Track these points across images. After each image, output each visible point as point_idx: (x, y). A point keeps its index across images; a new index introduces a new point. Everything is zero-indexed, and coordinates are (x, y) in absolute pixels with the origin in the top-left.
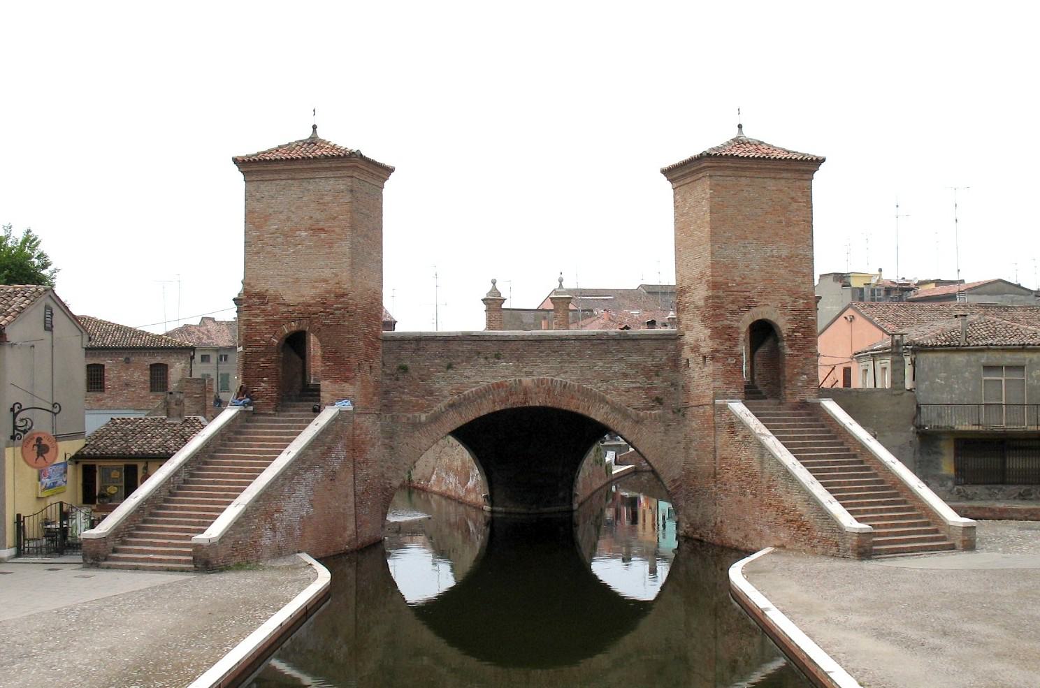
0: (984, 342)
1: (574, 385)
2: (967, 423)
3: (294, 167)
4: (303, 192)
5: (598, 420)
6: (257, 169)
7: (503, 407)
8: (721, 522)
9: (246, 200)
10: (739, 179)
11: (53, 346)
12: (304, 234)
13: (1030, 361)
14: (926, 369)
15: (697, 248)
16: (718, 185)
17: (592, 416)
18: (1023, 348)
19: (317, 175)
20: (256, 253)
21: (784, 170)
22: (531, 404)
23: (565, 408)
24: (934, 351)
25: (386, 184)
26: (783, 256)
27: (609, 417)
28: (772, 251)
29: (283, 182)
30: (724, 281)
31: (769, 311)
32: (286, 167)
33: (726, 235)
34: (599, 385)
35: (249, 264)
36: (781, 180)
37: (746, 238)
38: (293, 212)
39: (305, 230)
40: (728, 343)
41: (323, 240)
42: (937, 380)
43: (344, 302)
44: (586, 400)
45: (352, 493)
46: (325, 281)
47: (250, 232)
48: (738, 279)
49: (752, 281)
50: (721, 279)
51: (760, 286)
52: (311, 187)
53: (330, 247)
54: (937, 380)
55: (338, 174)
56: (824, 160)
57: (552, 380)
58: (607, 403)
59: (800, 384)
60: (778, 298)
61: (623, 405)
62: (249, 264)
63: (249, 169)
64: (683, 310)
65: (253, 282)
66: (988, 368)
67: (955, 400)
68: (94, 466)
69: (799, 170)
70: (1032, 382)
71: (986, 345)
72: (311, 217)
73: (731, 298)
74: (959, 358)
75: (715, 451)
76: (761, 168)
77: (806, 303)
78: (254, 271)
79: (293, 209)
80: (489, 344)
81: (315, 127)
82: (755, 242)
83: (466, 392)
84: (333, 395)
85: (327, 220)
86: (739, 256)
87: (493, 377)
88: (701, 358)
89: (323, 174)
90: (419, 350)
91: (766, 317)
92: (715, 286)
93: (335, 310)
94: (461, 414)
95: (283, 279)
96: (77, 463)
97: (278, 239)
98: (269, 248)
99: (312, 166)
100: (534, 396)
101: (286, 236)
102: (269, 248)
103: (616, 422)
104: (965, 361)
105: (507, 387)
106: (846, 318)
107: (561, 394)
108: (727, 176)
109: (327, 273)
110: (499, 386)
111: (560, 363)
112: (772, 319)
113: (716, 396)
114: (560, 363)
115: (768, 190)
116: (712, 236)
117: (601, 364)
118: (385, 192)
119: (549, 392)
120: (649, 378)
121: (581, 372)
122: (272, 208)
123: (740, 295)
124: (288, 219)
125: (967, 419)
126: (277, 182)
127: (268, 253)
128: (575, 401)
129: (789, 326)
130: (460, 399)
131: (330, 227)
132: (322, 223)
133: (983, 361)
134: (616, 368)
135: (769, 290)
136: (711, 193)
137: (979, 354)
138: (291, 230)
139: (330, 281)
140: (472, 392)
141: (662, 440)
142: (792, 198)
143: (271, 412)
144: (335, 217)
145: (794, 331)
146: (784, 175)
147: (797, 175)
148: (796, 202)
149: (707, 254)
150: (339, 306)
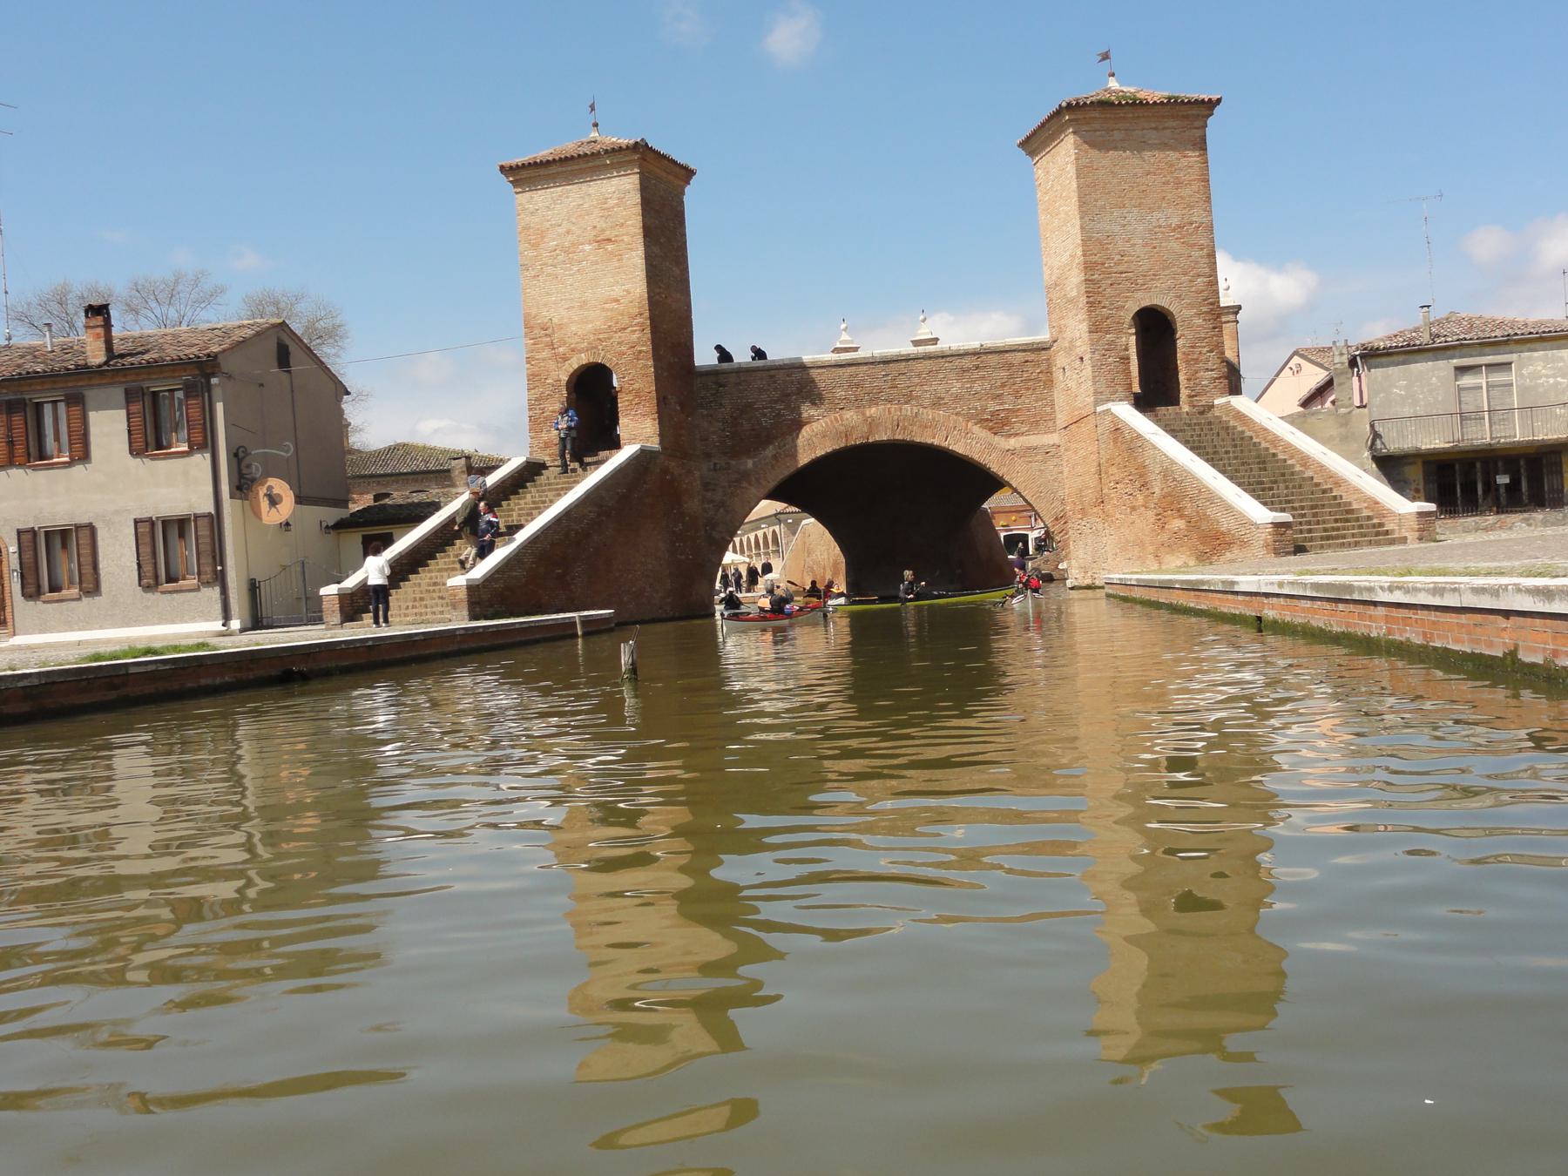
0: (1455, 338)
2: (1437, 441)
3: (569, 168)
11: (292, 391)
12: (587, 247)
14: (1380, 378)
15: (1064, 228)
18: (1508, 340)
24: (1388, 354)
25: (687, 189)
26: (1173, 226)
28: (1158, 220)
33: (1100, 203)
35: (528, 291)
39: (590, 244)
41: (611, 253)
46: (617, 301)
53: (619, 260)
56: (1219, 101)
62: (528, 291)
63: (518, 177)
65: (534, 311)
67: (1422, 413)
69: (1186, 117)
70: (1522, 381)
71: (1458, 340)
72: (595, 227)
79: (574, 220)
82: (1135, 210)
85: (612, 228)
86: (1117, 228)
92: (1089, 267)
98: (549, 269)
102: (549, 269)
106: (1291, 369)
108: (1095, 131)
109: (617, 291)
113: (1097, 403)
115: (1149, 144)
116: (1080, 206)
117: (959, 385)
118: (685, 199)
122: (548, 221)
124: (568, 232)
125: (1437, 435)
126: (552, 190)
127: (549, 275)
131: (616, 236)
132: (608, 233)
136: (1076, 153)
139: (622, 301)
141: (1040, 470)
144: (623, 224)
149: (1077, 230)
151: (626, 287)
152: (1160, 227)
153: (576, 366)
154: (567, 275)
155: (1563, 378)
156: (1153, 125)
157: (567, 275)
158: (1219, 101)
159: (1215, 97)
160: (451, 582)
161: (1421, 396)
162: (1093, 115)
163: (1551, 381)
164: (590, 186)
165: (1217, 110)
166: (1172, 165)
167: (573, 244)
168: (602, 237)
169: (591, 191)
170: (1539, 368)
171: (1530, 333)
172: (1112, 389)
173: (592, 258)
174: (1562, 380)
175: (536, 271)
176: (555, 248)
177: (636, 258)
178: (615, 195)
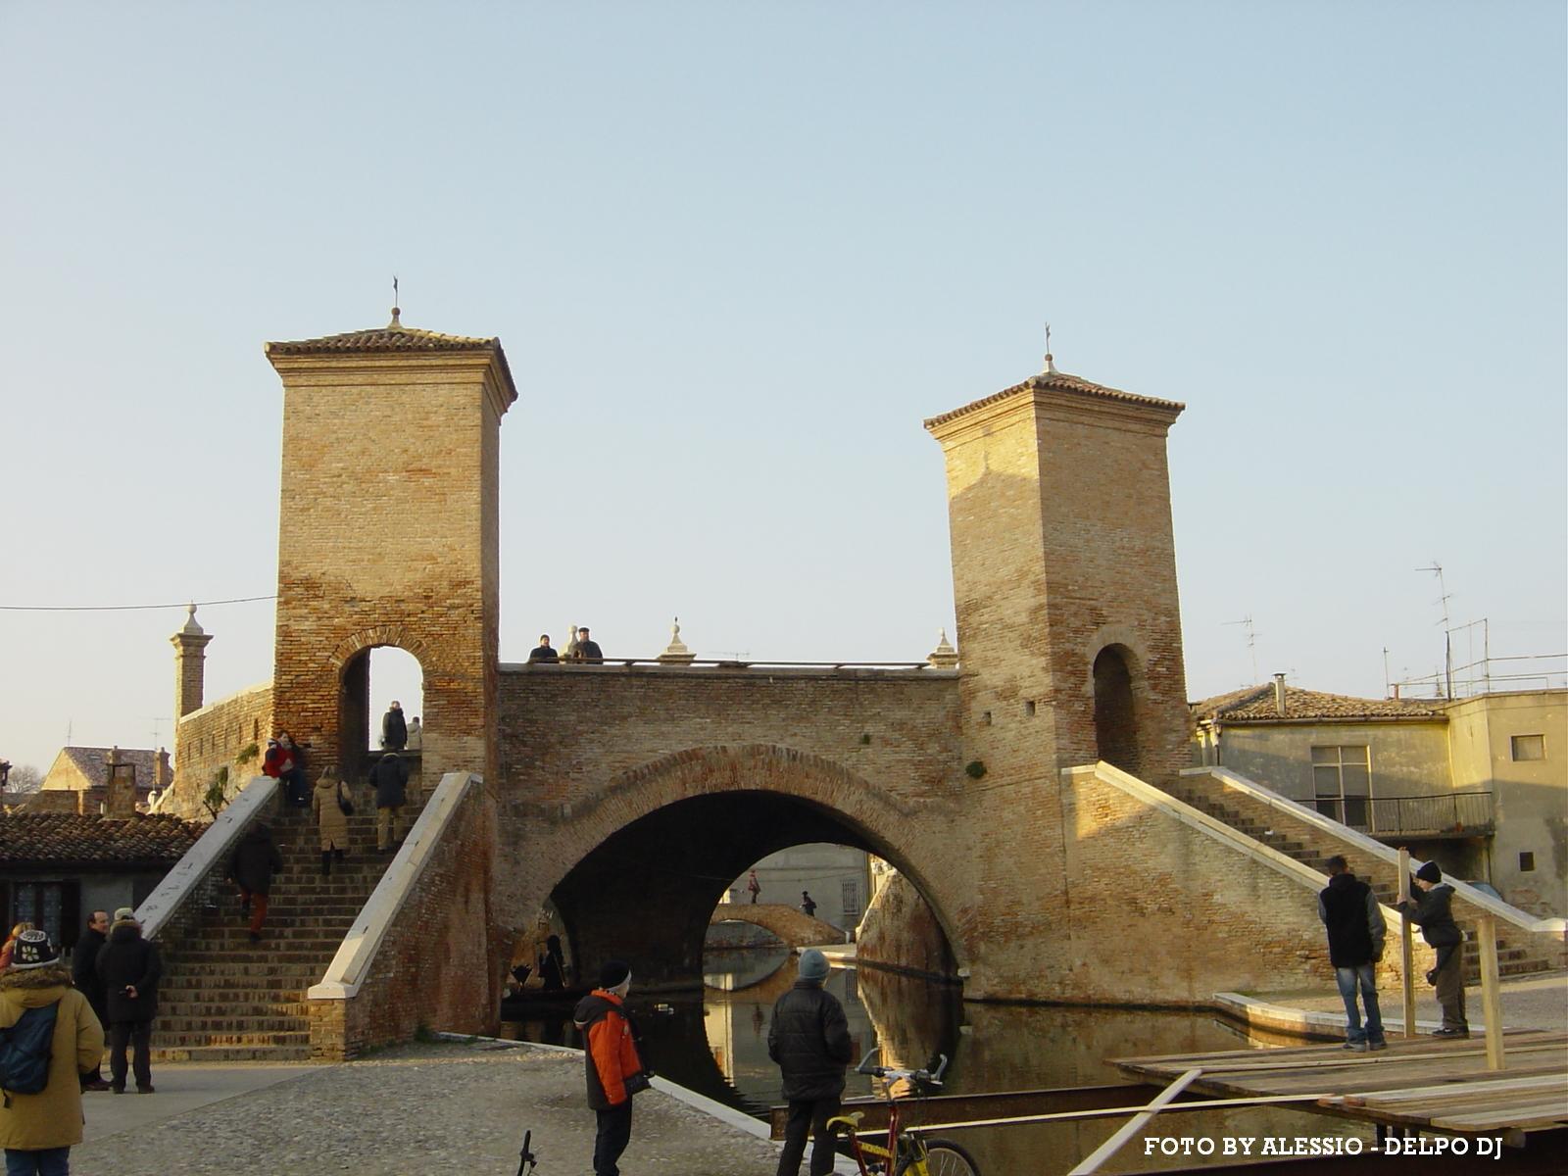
1: (808, 756)
5: (848, 812)
6: (311, 365)
7: (698, 792)
8: (1084, 965)
9: (287, 418)
10: (1074, 426)
12: (392, 478)
13: (1374, 739)
17: (839, 806)
18: (1366, 721)
19: (415, 377)
20: (302, 510)
21: (1132, 418)
22: (743, 786)
23: (796, 794)
25: (504, 418)
26: (1137, 549)
27: (865, 807)
28: (1121, 540)
29: (355, 390)
30: (1065, 581)
31: (1121, 631)
32: (369, 364)
33: (1064, 509)
34: (846, 756)
36: (1128, 434)
37: (1088, 518)
38: (374, 441)
39: (396, 472)
40: (1072, 679)
41: (430, 489)
42: (1251, 769)
43: (464, 594)
44: (828, 779)
45: (485, 933)
46: (432, 559)
47: (293, 473)
48: (1080, 580)
49: (1099, 584)
50: (1058, 578)
54: (1251, 769)
55: (458, 376)
56: (1183, 408)
57: (774, 747)
59: (1170, 747)
60: (1132, 611)
61: (884, 789)
62: (290, 528)
64: (974, 636)
69: (1149, 421)
73: (1073, 608)
75: (1065, 850)
77: (1167, 622)
78: (297, 542)
81: (396, 312)
82: (1099, 524)
84: (444, 757)
87: (680, 742)
88: (1022, 707)
89: (429, 377)
91: (1121, 640)
93: (449, 608)
94: (630, 804)
95: (354, 555)
97: (345, 486)
98: (329, 502)
99: (414, 363)
101: (359, 481)
103: (875, 815)
104: (1287, 740)
105: (704, 758)
108: (1058, 420)
109: (434, 545)
110: (690, 756)
111: (784, 720)
112: (1128, 645)
113: (1062, 763)
114: (784, 720)
117: (847, 722)
120: (921, 747)
121: (817, 733)
122: (335, 432)
123: (1084, 605)
127: (328, 510)
128: (810, 780)
129: (1150, 656)
130: (628, 778)
133: (1311, 740)
135: (1122, 599)
138: (369, 471)
148: (1147, 468)
150: (456, 601)
154: (354, 513)
155: (1416, 767)
157: (354, 513)
161: (1278, 777)
162: (1059, 402)
163: (1405, 769)
164: (404, 392)
165: (1182, 412)
168: (416, 465)
170: (1393, 755)
171: (1386, 715)
172: (1075, 746)
173: (397, 493)
174: (1416, 770)
178: (442, 410)
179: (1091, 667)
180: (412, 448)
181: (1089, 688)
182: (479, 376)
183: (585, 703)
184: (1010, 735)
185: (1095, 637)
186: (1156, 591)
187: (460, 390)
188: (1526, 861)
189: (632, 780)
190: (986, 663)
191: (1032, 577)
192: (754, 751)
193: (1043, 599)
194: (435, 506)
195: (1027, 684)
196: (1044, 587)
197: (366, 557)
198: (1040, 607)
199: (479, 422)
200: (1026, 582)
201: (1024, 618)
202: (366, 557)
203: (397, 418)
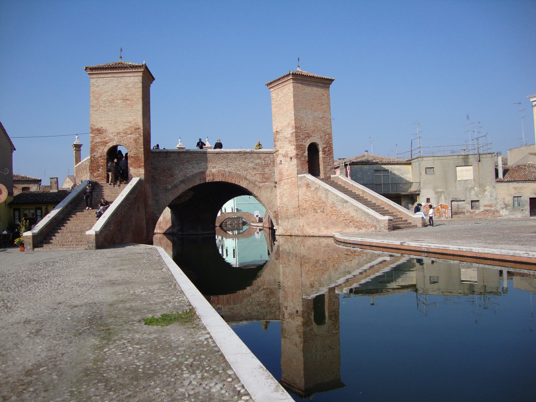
4: (119, 83)
12: (119, 101)
16: (296, 86)
21: (319, 82)
25: (152, 85)
30: (299, 126)
35: (93, 115)
39: (120, 100)
41: (129, 104)
43: (138, 132)
45: (145, 218)
46: (130, 122)
50: (298, 125)
51: (312, 129)
52: (122, 80)
55: (136, 74)
57: (224, 170)
58: (247, 180)
59: (328, 169)
60: (319, 134)
62: (93, 115)
64: (278, 141)
66: (376, 171)
68: (20, 208)
69: (324, 83)
72: (122, 94)
74: (366, 167)
76: (311, 81)
78: (95, 119)
80: (197, 155)
83: (188, 176)
88: (289, 159)
90: (167, 157)
96: (11, 208)
98: (103, 108)
100: (217, 177)
107: (229, 176)
109: (130, 119)
118: (151, 88)
119: (223, 175)
124: (111, 95)
126: (106, 78)
127: (102, 110)
131: (131, 98)
132: (128, 97)
134: (250, 165)
137: (373, 166)
138: (113, 100)
139: (132, 123)
140: (190, 175)
142: (322, 94)
143: (105, 183)
144: (134, 94)
145: (325, 148)
146: (320, 85)
147: (324, 85)
151: (134, 118)
152: (317, 117)
153: (111, 146)
156: (315, 84)
158: (334, 80)
159: (333, 79)
160: (88, 233)
161: (365, 178)
164: (122, 79)
166: (320, 98)
167: (113, 100)
168: (125, 98)
169: (122, 81)
173: (120, 105)
175: (97, 108)
176: (104, 100)
177: (139, 107)
179: (307, 148)
180: (124, 94)
181: (306, 154)
182: (141, 74)
183: (174, 159)
184: (286, 166)
185: (308, 141)
186: (326, 129)
187: (136, 78)
188: (428, 200)
189: (187, 179)
190: (280, 147)
191: (291, 125)
192: (219, 171)
193: (294, 131)
194: (131, 109)
195: (290, 153)
196: (294, 127)
197: (113, 122)
198: (294, 133)
199: (141, 86)
200: (290, 126)
201: (289, 136)
202: (113, 122)
203: (120, 86)
